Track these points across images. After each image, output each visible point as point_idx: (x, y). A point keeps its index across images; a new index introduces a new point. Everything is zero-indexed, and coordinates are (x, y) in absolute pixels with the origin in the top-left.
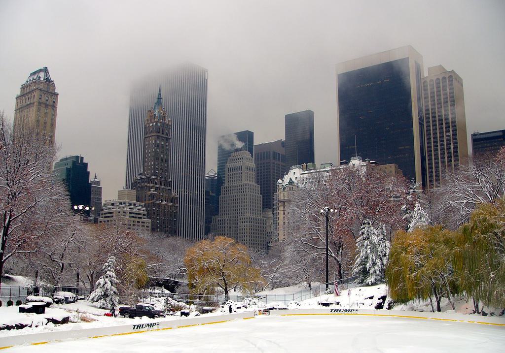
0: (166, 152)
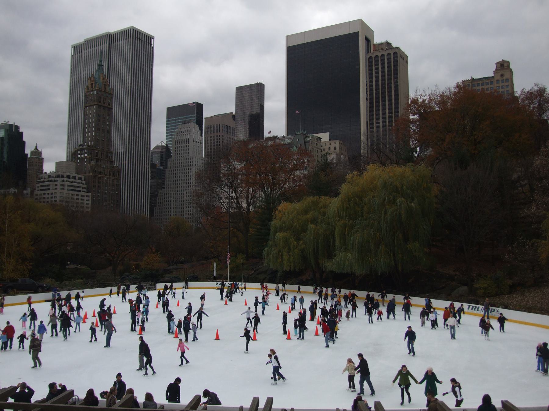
0: (108, 123)
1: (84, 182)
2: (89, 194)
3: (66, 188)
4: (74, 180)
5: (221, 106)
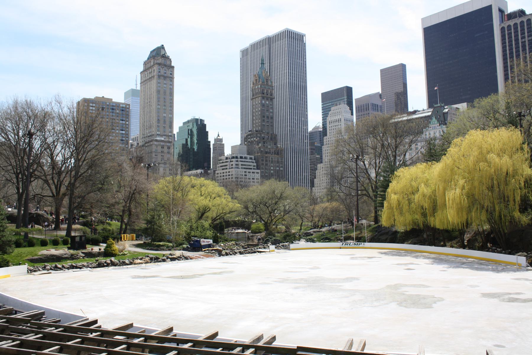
0: (271, 110)
1: (254, 161)
2: (259, 171)
3: (240, 166)
4: (246, 160)
5: (367, 85)
